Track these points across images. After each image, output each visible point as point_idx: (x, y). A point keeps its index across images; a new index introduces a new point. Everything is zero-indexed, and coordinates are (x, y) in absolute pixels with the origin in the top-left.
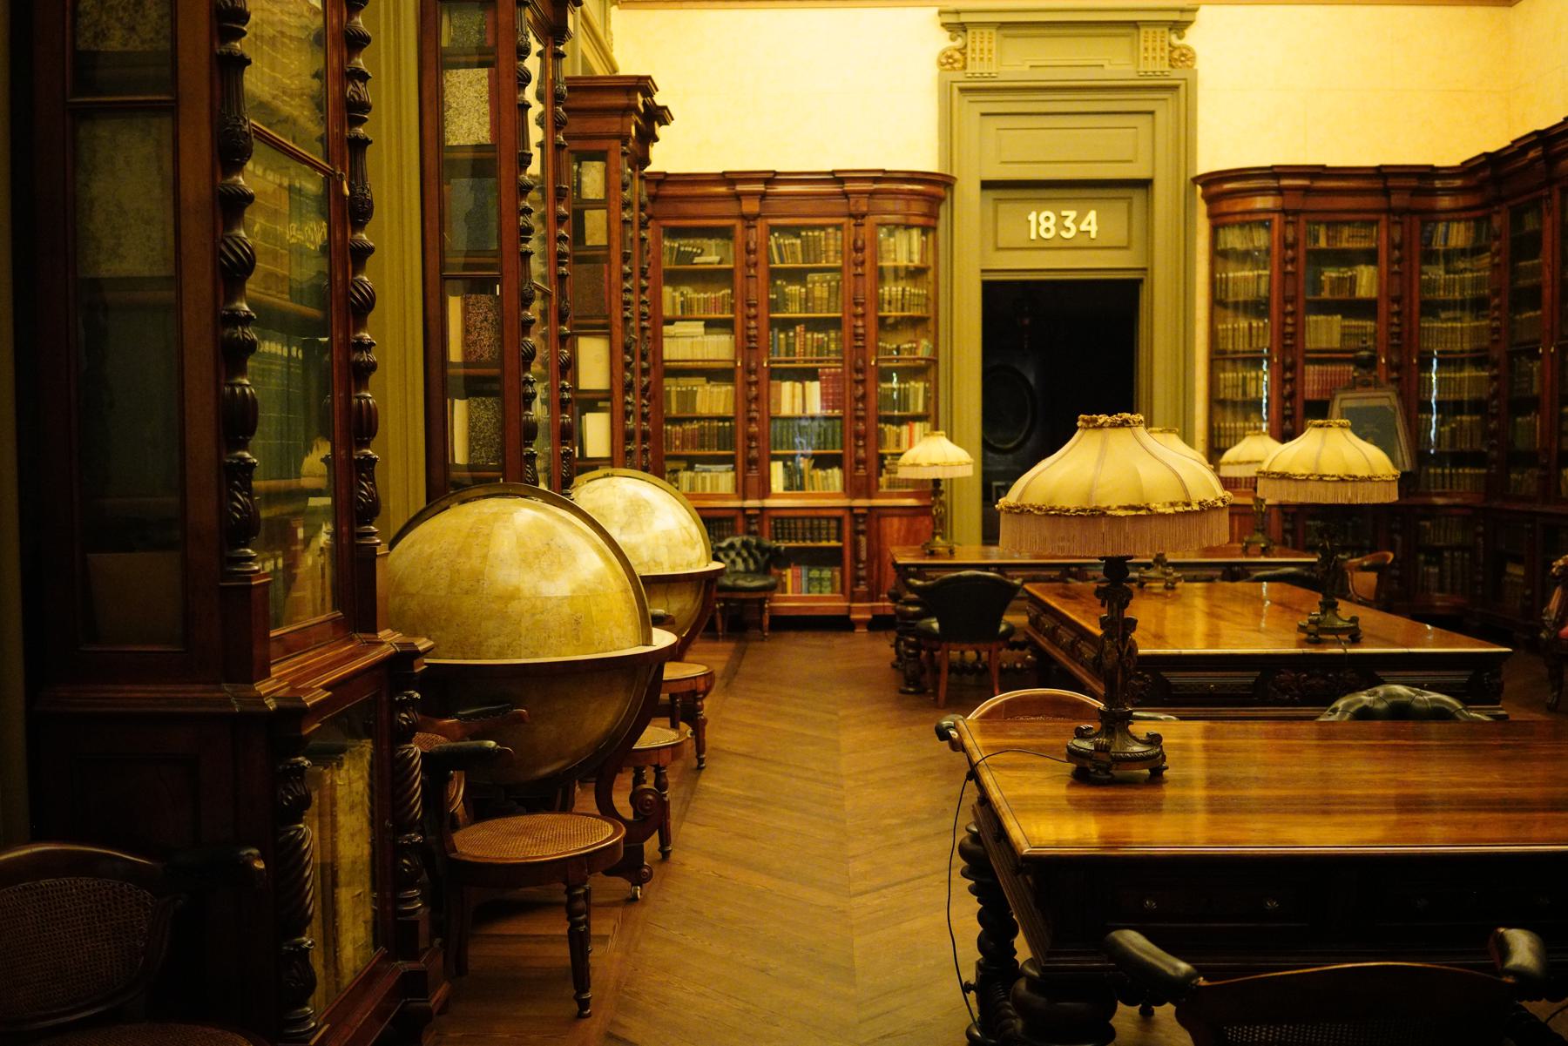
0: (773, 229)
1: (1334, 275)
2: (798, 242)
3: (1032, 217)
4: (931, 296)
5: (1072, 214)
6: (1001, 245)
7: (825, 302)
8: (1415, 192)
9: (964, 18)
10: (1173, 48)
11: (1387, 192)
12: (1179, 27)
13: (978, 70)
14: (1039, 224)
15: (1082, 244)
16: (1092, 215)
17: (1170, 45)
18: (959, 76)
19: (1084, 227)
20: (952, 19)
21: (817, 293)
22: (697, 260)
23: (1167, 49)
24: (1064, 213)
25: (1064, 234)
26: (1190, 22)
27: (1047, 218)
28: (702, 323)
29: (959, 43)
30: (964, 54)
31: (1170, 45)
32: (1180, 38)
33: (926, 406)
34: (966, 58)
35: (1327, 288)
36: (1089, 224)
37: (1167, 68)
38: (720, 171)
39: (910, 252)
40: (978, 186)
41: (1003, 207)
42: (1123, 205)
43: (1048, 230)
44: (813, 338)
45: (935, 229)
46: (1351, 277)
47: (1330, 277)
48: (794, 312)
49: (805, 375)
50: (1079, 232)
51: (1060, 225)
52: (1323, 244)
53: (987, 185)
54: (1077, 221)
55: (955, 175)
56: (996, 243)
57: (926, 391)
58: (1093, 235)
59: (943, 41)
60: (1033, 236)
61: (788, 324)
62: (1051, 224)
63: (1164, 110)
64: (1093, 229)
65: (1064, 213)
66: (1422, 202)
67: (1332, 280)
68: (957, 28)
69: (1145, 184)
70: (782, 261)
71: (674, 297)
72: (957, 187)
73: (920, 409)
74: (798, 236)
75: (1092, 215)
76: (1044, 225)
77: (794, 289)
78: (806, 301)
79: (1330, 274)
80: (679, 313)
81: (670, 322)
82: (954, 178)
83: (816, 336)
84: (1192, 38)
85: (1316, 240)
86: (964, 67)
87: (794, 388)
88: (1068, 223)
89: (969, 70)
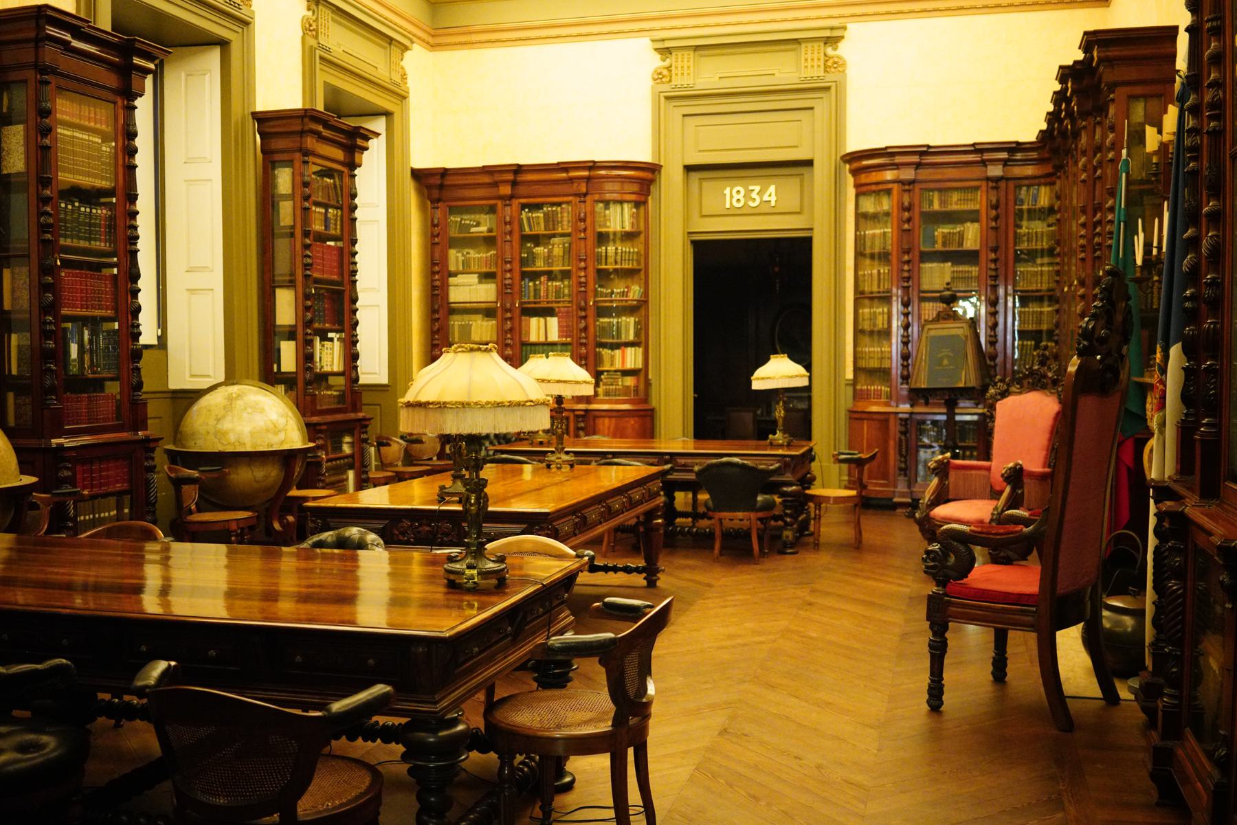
1: (946, 231)
3: (727, 191)
4: (642, 252)
5: (757, 188)
6: (704, 213)
7: (561, 259)
9: (668, 44)
11: (984, 163)
14: (732, 197)
16: (772, 189)
17: (825, 55)
18: (666, 87)
19: (766, 198)
20: (660, 45)
22: (473, 230)
24: (751, 188)
25: (752, 204)
26: (843, 37)
27: (738, 192)
28: (477, 275)
31: (825, 55)
32: (835, 49)
33: (637, 334)
35: (940, 241)
36: (770, 195)
38: (481, 165)
41: (705, 184)
42: (796, 180)
43: (738, 200)
45: (645, 203)
46: (959, 232)
47: (943, 233)
48: (540, 265)
49: (547, 312)
52: (936, 206)
53: (689, 169)
54: (760, 193)
55: (662, 164)
56: (701, 211)
59: (656, 62)
60: (728, 206)
61: (534, 276)
62: (740, 196)
63: (822, 105)
64: (773, 199)
65: (751, 188)
67: (945, 236)
68: (665, 52)
69: (809, 163)
71: (457, 257)
72: (663, 170)
73: (631, 337)
75: (772, 189)
76: (736, 197)
77: (540, 250)
78: (549, 258)
80: (461, 268)
81: (455, 275)
82: (661, 166)
83: (554, 284)
84: (843, 50)
85: (931, 203)
86: (670, 81)
87: (539, 322)
88: (754, 195)
89: (674, 83)
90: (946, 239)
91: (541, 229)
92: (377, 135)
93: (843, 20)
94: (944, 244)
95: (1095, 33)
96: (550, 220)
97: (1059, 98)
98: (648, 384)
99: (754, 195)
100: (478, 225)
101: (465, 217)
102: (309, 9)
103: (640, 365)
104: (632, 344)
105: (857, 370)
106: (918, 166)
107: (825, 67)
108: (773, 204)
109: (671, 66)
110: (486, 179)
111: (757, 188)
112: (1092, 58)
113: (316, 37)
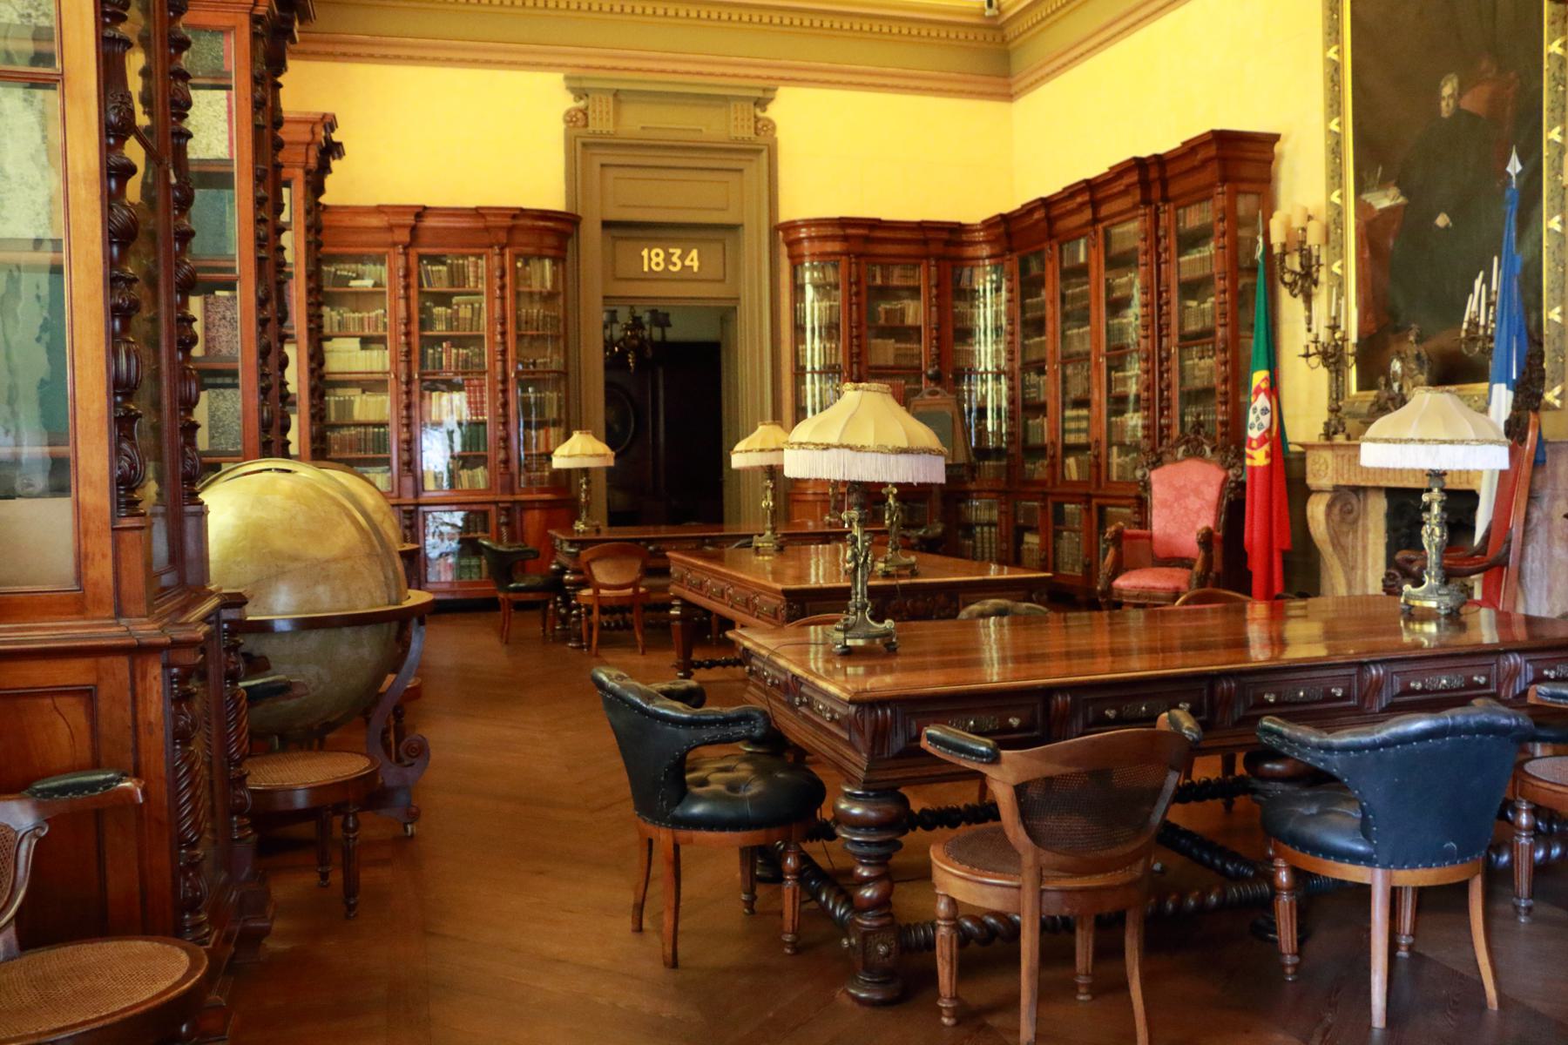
0: (421, 257)
2: (444, 269)
3: (645, 253)
4: (561, 316)
5: (678, 252)
6: (620, 275)
7: (468, 322)
8: (947, 243)
9: (586, 84)
10: (757, 119)
11: (925, 242)
12: (761, 103)
13: (598, 129)
15: (686, 276)
16: (694, 253)
17: (755, 117)
18: (582, 131)
19: (687, 263)
20: (576, 84)
21: (461, 314)
22: (353, 283)
23: (753, 120)
24: (671, 251)
25: (671, 268)
26: (772, 99)
27: (657, 255)
28: (358, 340)
29: (582, 104)
30: (586, 115)
32: (764, 110)
34: (587, 118)
35: (883, 316)
37: (753, 136)
40: (599, 225)
41: (619, 243)
42: (719, 247)
43: (658, 264)
44: (458, 355)
45: (564, 260)
48: (440, 329)
50: (683, 266)
52: (879, 281)
53: (607, 225)
54: (682, 258)
55: (579, 213)
57: (559, 399)
58: (695, 269)
59: (568, 102)
60: (646, 269)
61: (438, 340)
62: (660, 259)
64: (696, 264)
65: (671, 251)
66: (952, 251)
67: (887, 312)
68: (580, 93)
69: (733, 228)
70: (429, 285)
72: (583, 225)
74: (444, 263)
75: (694, 253)
76: (655, 260)
77: (439, 311)
79: (883, 307)
80: (336, 329)
81: (329, 338)
83: (461, 351)
84: (773, 112)
85: (874, 277)
86: (586, 125)
88: (675, 259)
89: (590, 129)
91: (442, 287)
93: (773, 82)
94: (886, 319)
96: (457, 276)
99: (675, 259)
100: (359, 277)
101: (342, 266)
107: (756, 128)
109: (587, 108)
110: (945, 236)
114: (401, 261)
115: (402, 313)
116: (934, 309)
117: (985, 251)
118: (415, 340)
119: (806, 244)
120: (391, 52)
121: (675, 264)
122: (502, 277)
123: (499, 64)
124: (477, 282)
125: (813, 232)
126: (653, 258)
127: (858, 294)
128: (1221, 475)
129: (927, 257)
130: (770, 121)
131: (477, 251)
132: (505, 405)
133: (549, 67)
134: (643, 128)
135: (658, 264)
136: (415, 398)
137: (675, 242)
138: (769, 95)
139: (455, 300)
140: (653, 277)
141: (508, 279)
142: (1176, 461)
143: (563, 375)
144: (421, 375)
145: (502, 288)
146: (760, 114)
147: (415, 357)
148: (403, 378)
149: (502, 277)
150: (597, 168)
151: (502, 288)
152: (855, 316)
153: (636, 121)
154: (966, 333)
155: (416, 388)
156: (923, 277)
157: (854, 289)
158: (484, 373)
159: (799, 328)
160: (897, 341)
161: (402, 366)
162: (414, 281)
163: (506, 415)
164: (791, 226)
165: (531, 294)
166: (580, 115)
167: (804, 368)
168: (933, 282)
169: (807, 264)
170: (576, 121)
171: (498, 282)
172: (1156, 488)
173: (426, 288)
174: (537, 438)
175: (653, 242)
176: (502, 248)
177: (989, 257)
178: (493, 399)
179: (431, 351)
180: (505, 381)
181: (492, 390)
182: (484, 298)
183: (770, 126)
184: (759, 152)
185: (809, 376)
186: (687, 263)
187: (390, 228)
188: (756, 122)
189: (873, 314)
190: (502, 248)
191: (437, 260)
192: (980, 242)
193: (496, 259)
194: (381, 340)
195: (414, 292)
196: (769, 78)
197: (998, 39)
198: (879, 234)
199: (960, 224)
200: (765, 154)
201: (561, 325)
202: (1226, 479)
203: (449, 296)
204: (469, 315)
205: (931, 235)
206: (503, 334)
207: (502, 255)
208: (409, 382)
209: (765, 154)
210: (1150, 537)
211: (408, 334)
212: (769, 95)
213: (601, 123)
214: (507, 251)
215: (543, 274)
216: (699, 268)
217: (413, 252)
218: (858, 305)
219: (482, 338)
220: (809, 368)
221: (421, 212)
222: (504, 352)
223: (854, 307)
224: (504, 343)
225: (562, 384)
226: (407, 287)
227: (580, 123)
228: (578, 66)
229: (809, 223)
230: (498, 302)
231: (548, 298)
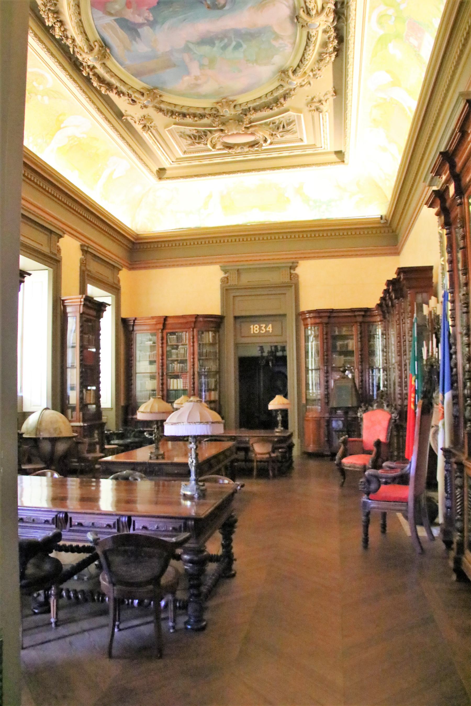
1: (341, 343)
2: (175, 336)
3: (252, 327)
4: (217, 351)
5: (264, 325)
6: (243, 335)
9: (227, 268)
10: (291, 274)
11: (355, 316)
12: (293, 268)
14: (254, 329)
15: (267, 335)
19: (268, 329)
21: (181, 352)
23: (289, 274)
24: (262, 325)
25: (262, 332)
26: (297, 266)
27: (256, 327)
29: (226, 275)
30: (228, 279)
31: (290, 273)
32: (294, 270)
33: (216, 386)
37: (289, 280)
39: (209, 339)
41: (243, 324)
43: (256, 331)
45: (218, 331)
48: (174, 357)
49: (177, 377)
50: (266, 331)
51: (260, 328)
52: (337, 333)
53: (236, 318)
54: (265, 328)
55: (225, 315)
57: (216, 381)
58: (271, 332)
59: (222, 275)
60: (252, 332)
61: (173, 361)
62: (257, 329)
64: (271, 330)
65: (262, 325)
67: (340, 345)
69: (285, 315)
70: (170, 342)
73: (213, 387)
76: (255, 329)
77: (174, 351)
79: (339, 343)
84: (298, 271)
85: (335, 332)
86: (228, 282)
89: (229, 284)
90: (342, 346)
91: (174, 343)
92: (109, 305)
93: (297, 260)
94: (340, 348)
95: (402, 268)
96: (179, 339)
97: (386, 292)
98: (220, 406)
102: (83, 255)
103: (217, 398)
104: (214, 390)
105: (307, 400)
106: (329, 317)
107: (291, 277)
108: (271, 332)
111: (264, 325)
112: (400, 278)
113: (85, 266)
114: (160, 335)
115: (160, 352)
116: (359, 343)
117: (378, 318)
118: (165, 361)
119: (309, 320)
120: (154, 265)
121: (263, 330)
122: (193, 338)
123: (199, 264)
124: (186, 341)
125: (312, 315)
126: (255, 329)
127: (326, 339)
128: (389, 417)
129: (356, 322)
130: (296, 274)
131: (181, 330)
132: (194, 383)
133: (212, 263)
134: (248, 282)
135: (256, 331)
136: (165, 381)
137: (263, 322)
138: (295, 265)
139: (180, 347)
140: (255, 336)
141: (195, 340)
142: (373, 410)
143: (218, 372)
144: (166, 374)
145: (193, 342)
146: (292, 272)
147: (165, 367)
148: (160, 374)
149: (193, 338)
150: (232, 298)
151: (193, 342)
152: (325, 347)
153: (246, 279)
154: (372, 353)
155: (165, 377)
156: (355, 330)
157: (325, 336)
158: (187, 372)
159: (307, 353)
160: (344, 357)
161: (160, 371)
162: (165, 341)
163: (194, 387)
164: (303, 313)
165: (206, 344)
166: (226, 279)
167: (308, 368)
168: (359, 332)
169: (309, 328)
170: (225, 281)
171: (192, 340)
172: (364, 421)
173: (169, 344)
174: (205, 395)
175: (254, 322)
176: (193, 329)
177: (381, 321)
178: (190, 382)
179: (171, 365)
180: (194, 375)
181: (190, 378)
182: (187, 346)
183: (297, 276)
184: (291, 286)
185: (310, 372)
186: (268, 329)
187: (156, 324)
188: (291, 275)
189: (334, 347)
190: (193, 329)
191: (173, 333)
192: (377, 315)
193: (191, 333)
194: (155, 362)
195: (165, 345)
196: (296, 258)
197: (391, 231)
198: (335, 314)
199: (368, 308)
200: (293, 287)
201: (218, 355)
202: (391, 419)
203: (178, 346)
204: (183, 352)
205: (357, 313)
206: (193, 358)
207: (193, 331)
208: (163, 375)
209: (293, 287)
210: (362, 441)
211: (162, 359)
212: (295, 265)
213: (233, 281)
214: (195, 330)
215: (209, 337)
216: (272, 331)
217: (165, 332)
218: (327, 343)
219: (186, 360)
220: (310, 368)
221: (166, 318)
222: (194, 365)
223: (325, 344)
224: (194, 362)
225: (218, 376)
226: (162, 343)
227: (225, 282)
228: (225, 262)
229: (310, 312)
230: (192, 348)
231: (213, 344)
